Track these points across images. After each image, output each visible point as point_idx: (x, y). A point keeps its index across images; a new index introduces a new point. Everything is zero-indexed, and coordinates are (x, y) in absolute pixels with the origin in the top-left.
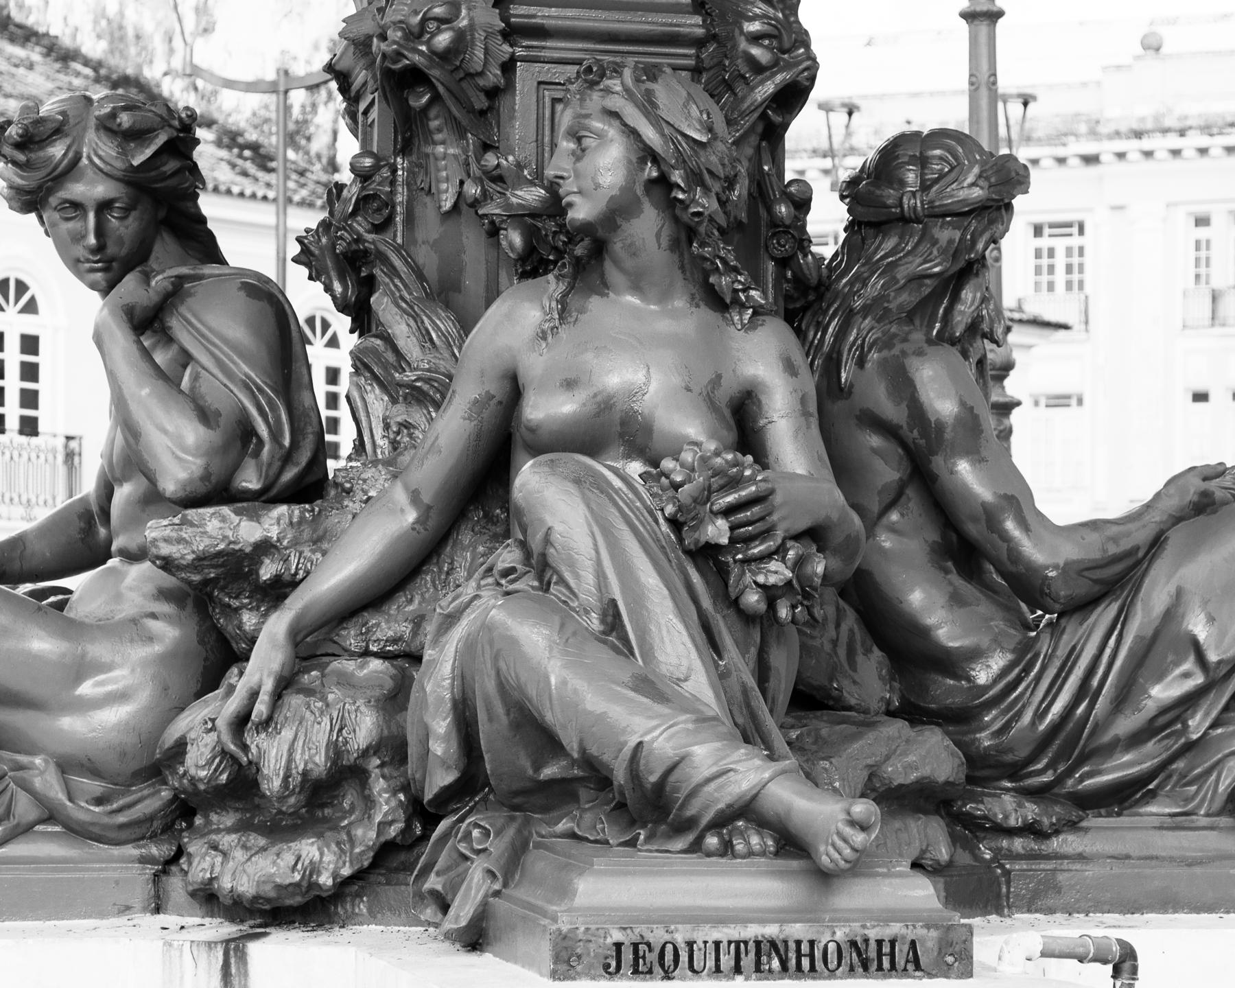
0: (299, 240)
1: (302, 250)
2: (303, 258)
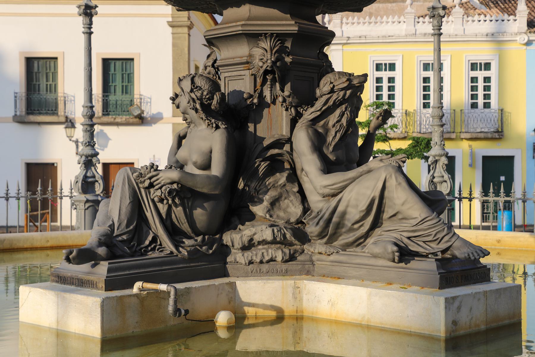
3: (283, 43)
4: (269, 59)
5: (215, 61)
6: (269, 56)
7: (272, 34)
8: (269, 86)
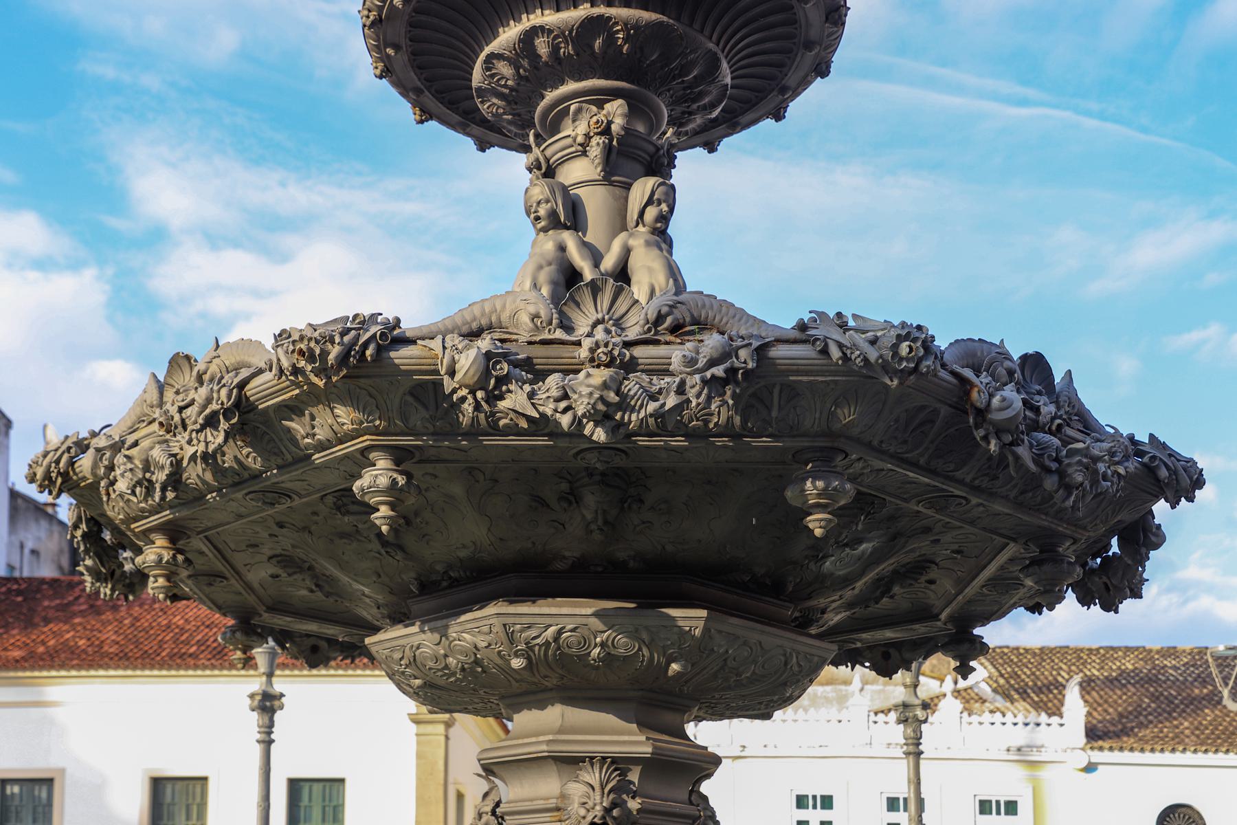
3: (623, 773)
4: (599, 803)
5: (498, 804)
6: (598, 798)
7: (604, 758)
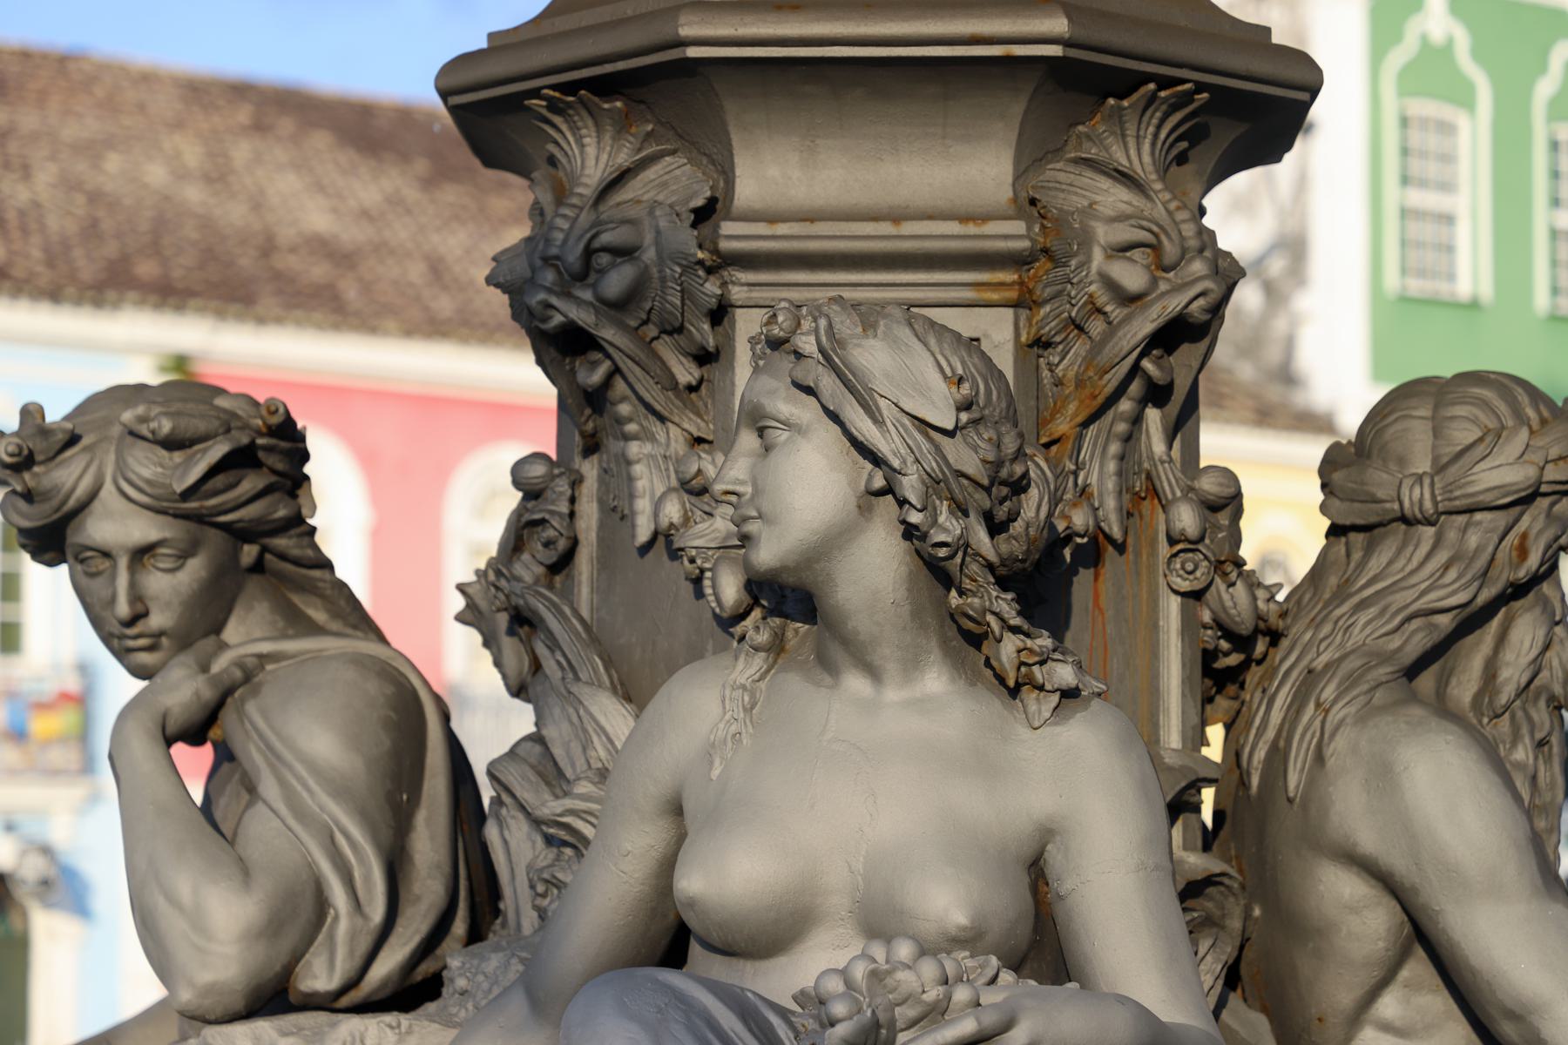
0: (461, 588)
1: (468, 605)
2: (469, 616)
8: (1121, 427)
